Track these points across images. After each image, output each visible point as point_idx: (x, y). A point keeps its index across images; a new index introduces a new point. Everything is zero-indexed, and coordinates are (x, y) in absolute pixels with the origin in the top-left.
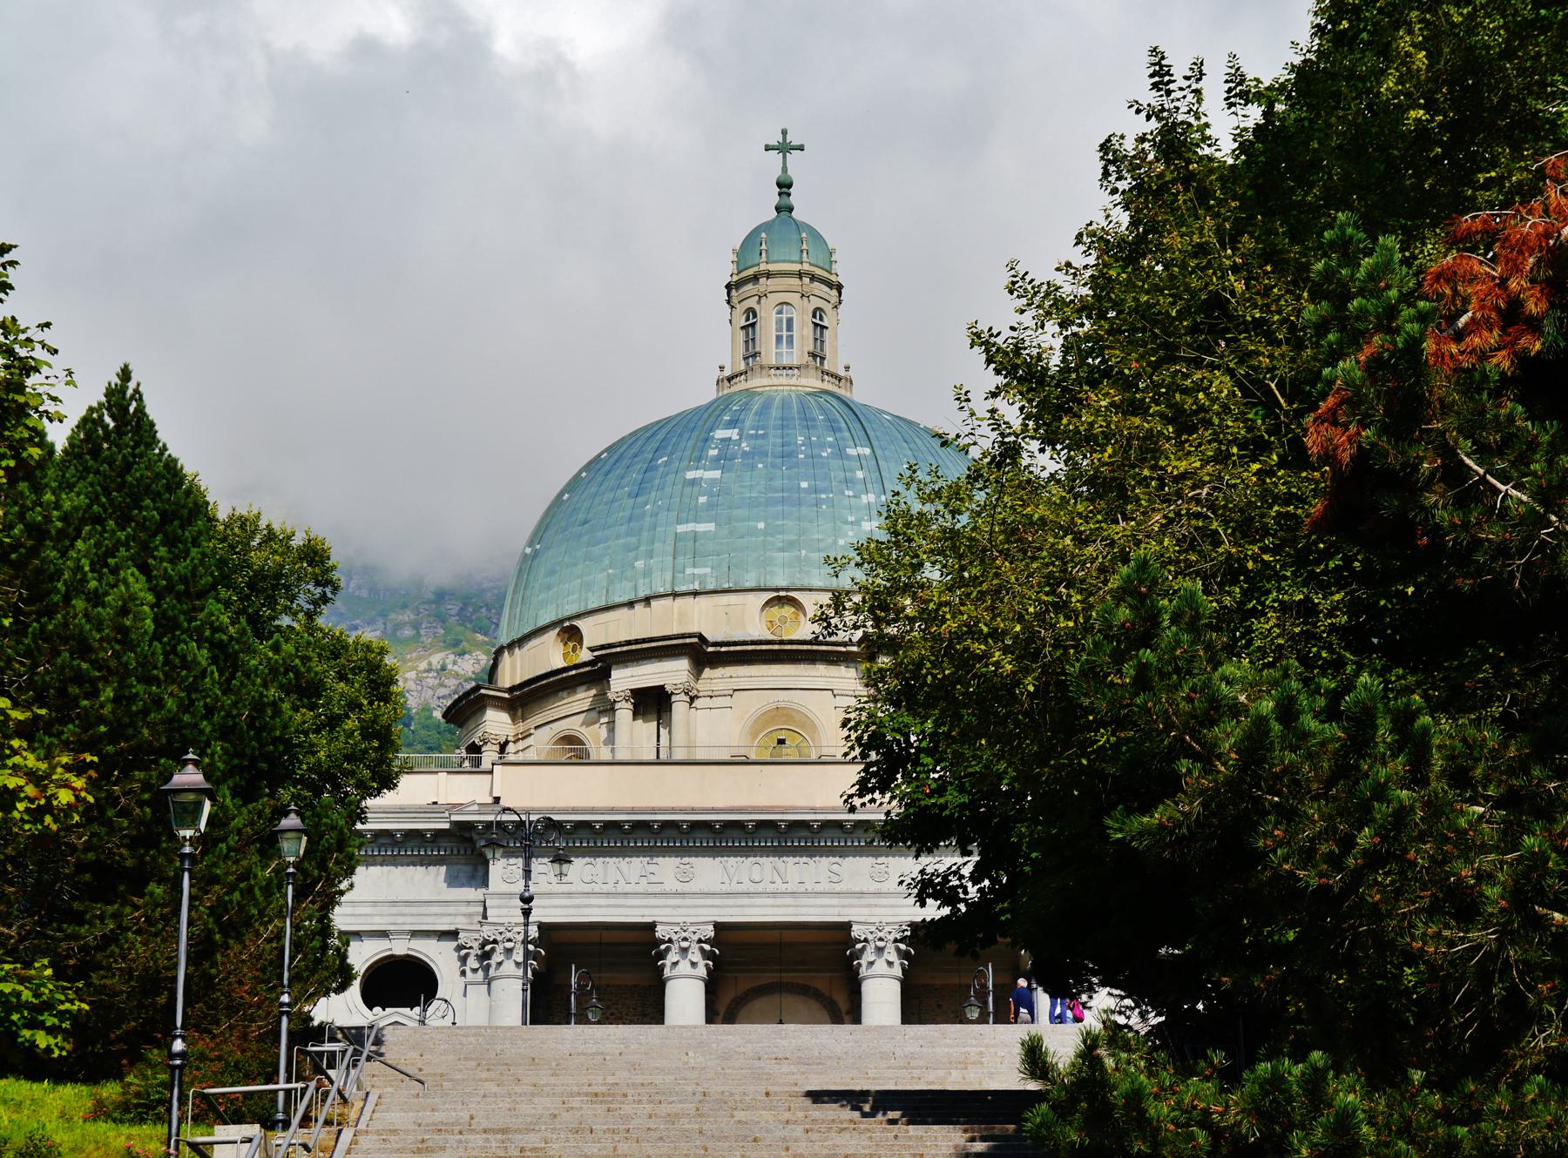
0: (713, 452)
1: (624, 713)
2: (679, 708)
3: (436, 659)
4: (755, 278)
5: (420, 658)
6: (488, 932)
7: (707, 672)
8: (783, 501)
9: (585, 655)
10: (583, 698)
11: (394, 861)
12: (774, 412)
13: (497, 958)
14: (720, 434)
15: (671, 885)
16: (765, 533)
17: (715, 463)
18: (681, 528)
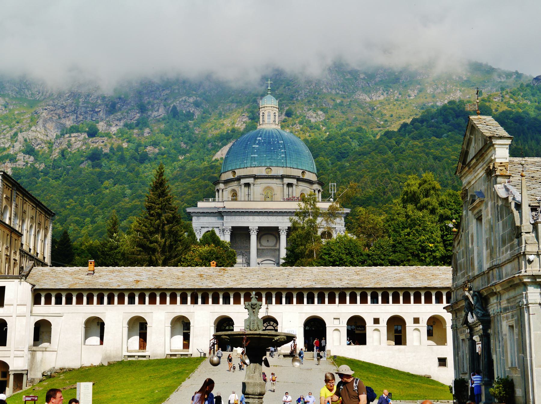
0: (257, 142)
1: (243, 186)
2: (252, 186)
3: (184, 98)
4: (264, 107)
5: (180, 98)
6: (224, 228)
7: (256, 180)
8: (269, 151)
9: (236, 177)
10: (236, 183)
11: (209, 216)
12: (267, 134)
13: (225, 232)
14: (258, 138)
15: (251, 221)
16: (266, 157)
17: (257, 144)
18: (252, 156)
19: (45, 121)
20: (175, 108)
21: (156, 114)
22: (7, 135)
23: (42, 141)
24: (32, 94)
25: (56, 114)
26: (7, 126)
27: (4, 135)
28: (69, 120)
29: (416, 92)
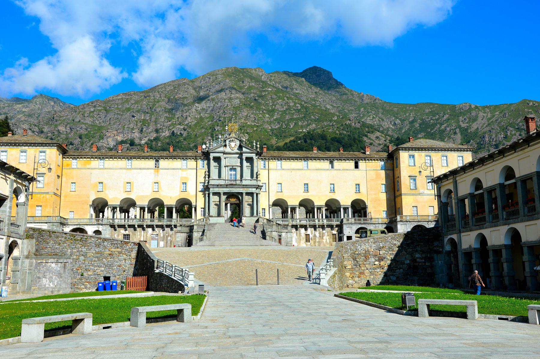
19: (108, 138)
20: (173, 132)
21: (164, 134)
22: (88, 144)
23: (106, 147)
24: (100, 123)
25: (113, 134)
26: (87, 140)
27: (86, 144)
28: (119, 137)
29: (293, 124)
